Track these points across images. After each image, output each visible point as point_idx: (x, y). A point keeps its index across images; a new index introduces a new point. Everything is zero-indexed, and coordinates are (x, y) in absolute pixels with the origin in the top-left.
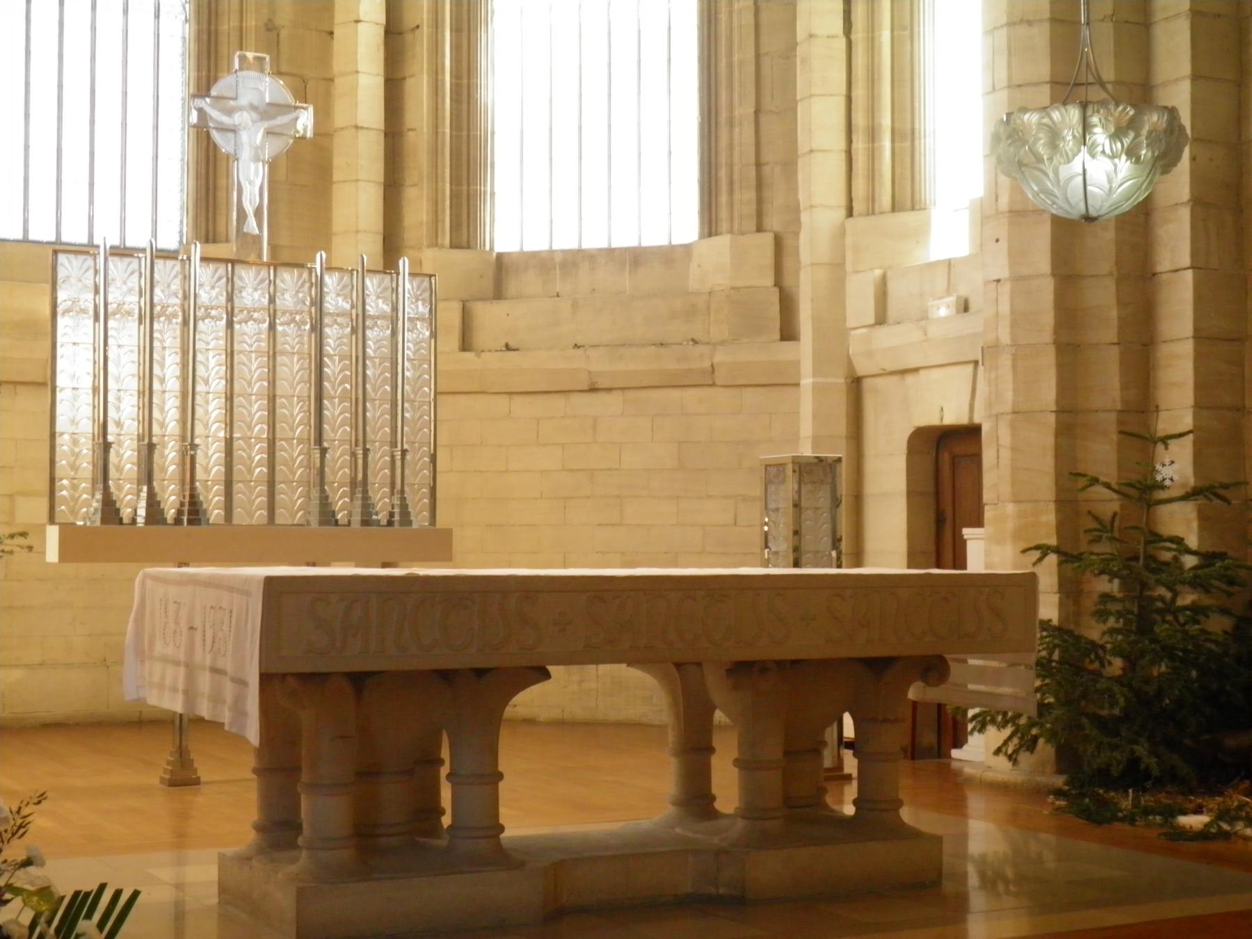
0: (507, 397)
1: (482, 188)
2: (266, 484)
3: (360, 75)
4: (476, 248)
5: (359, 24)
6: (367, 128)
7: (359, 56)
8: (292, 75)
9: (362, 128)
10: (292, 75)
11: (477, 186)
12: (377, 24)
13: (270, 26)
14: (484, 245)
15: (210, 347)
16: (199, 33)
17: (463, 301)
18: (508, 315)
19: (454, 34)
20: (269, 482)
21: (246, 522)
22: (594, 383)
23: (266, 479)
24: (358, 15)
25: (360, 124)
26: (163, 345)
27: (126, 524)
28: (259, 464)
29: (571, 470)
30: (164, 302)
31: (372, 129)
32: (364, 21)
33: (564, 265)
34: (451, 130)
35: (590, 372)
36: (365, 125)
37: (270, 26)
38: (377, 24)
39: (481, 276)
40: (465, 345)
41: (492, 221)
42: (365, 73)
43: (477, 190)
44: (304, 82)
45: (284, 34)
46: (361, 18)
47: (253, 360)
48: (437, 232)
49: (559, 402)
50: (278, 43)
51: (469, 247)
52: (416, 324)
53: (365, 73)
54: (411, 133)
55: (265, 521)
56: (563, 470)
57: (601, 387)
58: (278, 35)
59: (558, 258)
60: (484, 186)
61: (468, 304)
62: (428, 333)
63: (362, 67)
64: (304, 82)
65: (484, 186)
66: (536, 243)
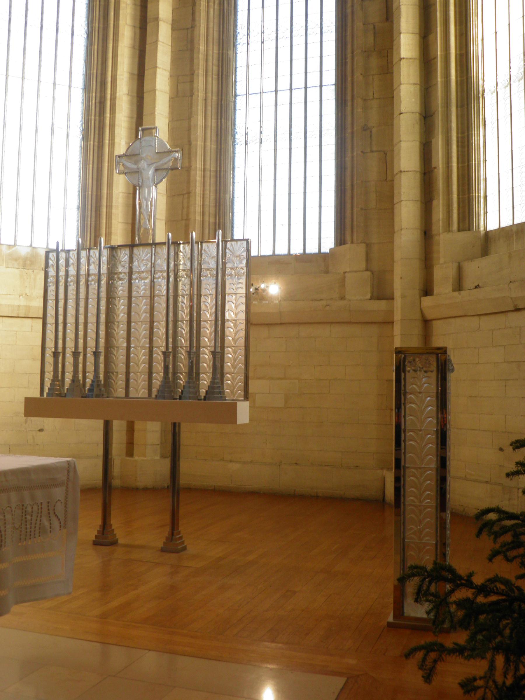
0: (477, 318)
1: (477, 194)
3: (402, 142)
4: (473, 230)
5: (401, 115)
6: (407, 171)
7: (401, 132)
8: (379, 151)
9: (404, 171)
10: (379, 151)
11: (473, 193)
12: (413, 113)
13: (365, 128)
14: (479, 228)
17: (458, 262)
18: (479, 267)
19: (459, 108)
22: (515, 306)
24: (400, 110)
25: (402, 169)
28: (143, 362)
29: (508, 362)
31: (410, 171)
32: (404, 113)
33: (517, 233)
34: (458, 163)
35: (511, 298)
36: (406, 170)
37: (365, 128)
38: (413, 113)
39: (474, 246)
40: (459, 286)
41: (486, 212)
42: (405, 141)
43: (473, 196)
44: (385, 154)
45: (374, 130)
46: (402, 112)
48: (449, 224)
49: (501, 318)
50: (371, 136)
51: (469, 230)
53: (405, 141)
54: (436, 170)
56: (505, 362)
57: (520, 307)
58: (371, 132)
59: (514, 229)
60: (478, 193)
61: (461, 264)
63: (403, 137)
64: (385, 154)
65: (478, 193)
66: (506, 222)
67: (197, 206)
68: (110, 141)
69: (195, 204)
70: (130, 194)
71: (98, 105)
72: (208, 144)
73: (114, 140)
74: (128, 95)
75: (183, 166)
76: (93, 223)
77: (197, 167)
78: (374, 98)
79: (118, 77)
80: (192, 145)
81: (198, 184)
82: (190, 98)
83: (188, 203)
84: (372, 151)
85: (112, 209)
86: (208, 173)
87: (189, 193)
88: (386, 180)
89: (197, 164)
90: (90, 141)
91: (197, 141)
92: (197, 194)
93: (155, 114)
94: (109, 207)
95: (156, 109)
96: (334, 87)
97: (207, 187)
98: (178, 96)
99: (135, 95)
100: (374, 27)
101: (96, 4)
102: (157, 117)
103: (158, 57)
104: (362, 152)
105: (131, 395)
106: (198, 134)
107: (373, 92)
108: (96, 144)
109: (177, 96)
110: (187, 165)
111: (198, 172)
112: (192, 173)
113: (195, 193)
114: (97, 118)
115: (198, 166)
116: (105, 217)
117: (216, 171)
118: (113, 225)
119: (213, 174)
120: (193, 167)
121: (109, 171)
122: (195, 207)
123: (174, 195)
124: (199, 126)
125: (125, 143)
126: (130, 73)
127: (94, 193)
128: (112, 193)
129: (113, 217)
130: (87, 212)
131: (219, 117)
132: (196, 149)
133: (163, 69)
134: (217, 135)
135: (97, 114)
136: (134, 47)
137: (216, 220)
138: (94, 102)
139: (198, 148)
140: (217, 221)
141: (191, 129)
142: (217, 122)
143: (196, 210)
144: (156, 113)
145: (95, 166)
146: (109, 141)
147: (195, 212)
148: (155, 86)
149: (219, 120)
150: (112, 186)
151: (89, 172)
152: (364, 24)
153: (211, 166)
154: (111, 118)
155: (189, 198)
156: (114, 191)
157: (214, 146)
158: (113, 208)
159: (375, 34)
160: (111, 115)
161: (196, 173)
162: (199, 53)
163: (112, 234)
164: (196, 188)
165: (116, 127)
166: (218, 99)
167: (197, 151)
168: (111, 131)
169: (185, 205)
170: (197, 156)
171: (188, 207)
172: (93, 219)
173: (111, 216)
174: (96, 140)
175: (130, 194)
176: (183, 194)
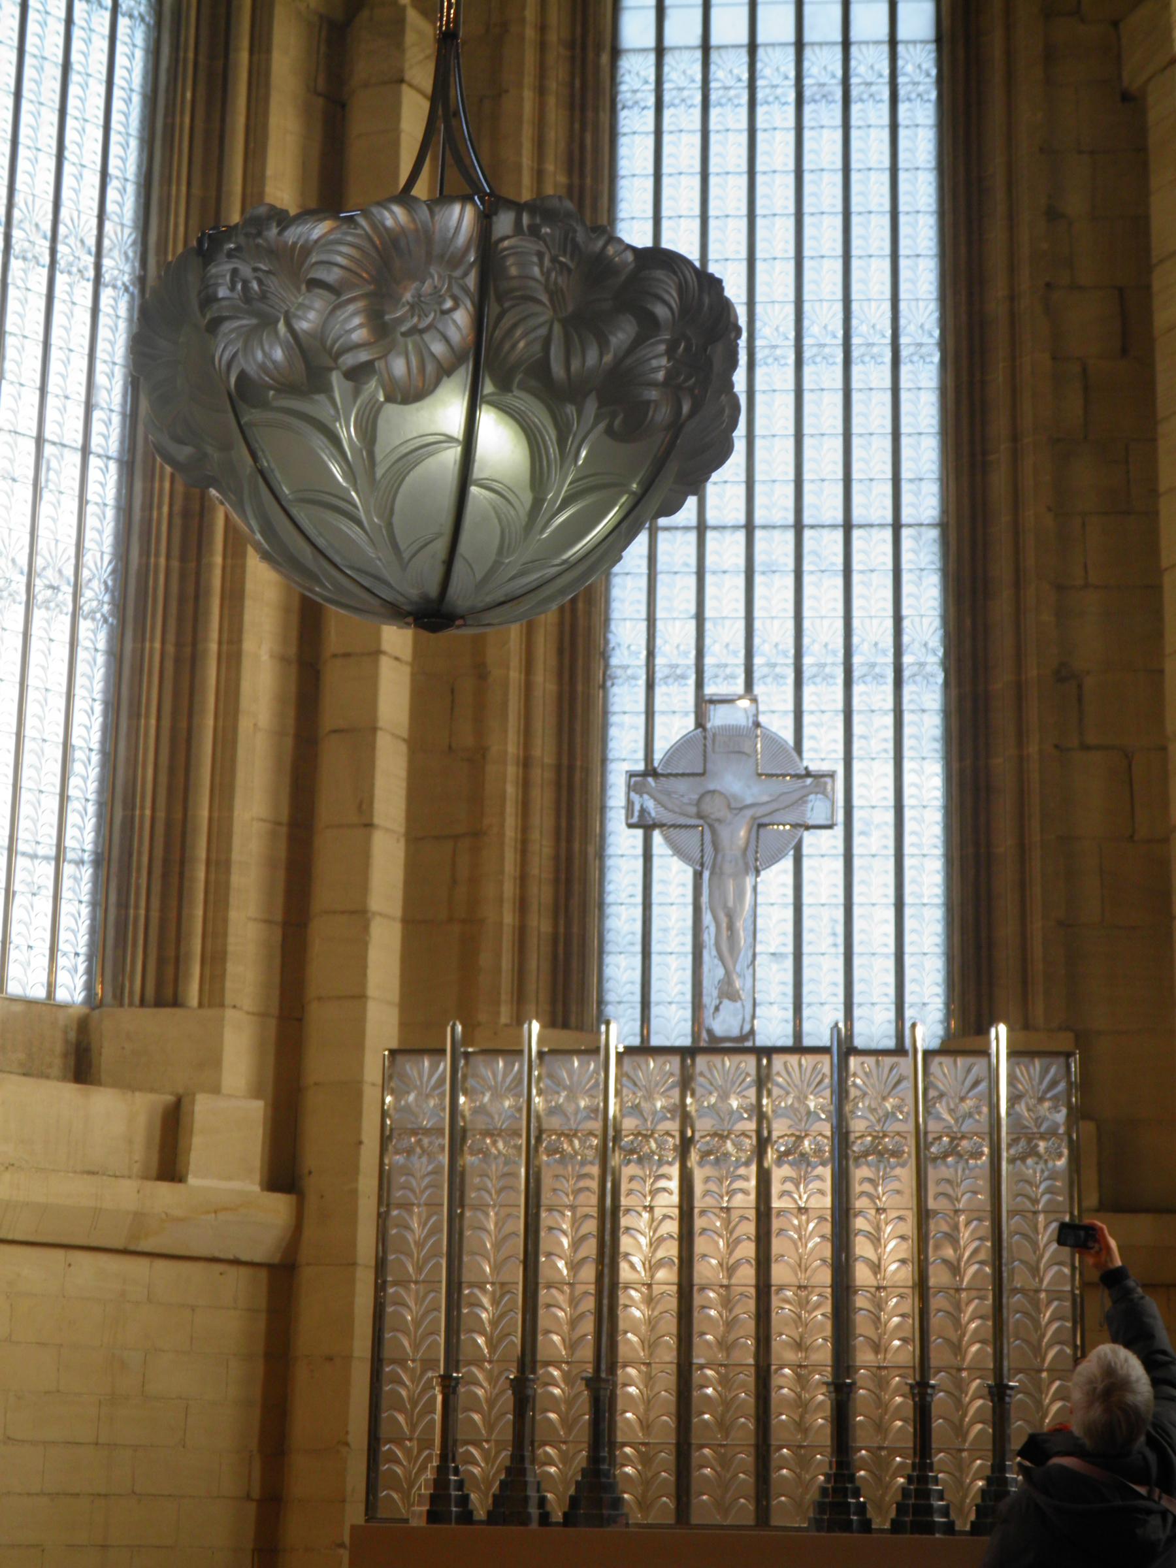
2: (752, 1450)
13: (1064, 675)
15: (961, 1206)
16: (961, 698)
20: (757, 1447)
21: (718, 1519)
23: (752, 1441)
26: (875, 1203)
27: (481, 1522)
30: (955, 1129)
37: (1064, 675)
47: (1041, 1226)
50: (1080, 699)
52: (1037, 1146)
55: (750, 1520)
58: (1080, 687)
62: (1061, 1163)
68: (224, 647)
69: (502, 872)
70: (279, 824)
71: (177, 521)
73: (239, 641)
76: (155, 915)
77: (505, 752)
78: (1086, 586)
84: (1085, 747)
85: (228, 871)
87: (477, 834)
88: (1132, 837)
89: (506, 744)
90: (152, 640)
91: (508, 668)
94: (220, 864)
96: (934, 533)
100: (1084, 370)
101: (178, 191)
104: (1056, 746)
105: (776, 1521)
107: (1085, 566)
108: (171, 649)
112: (491, 769)
113: (501, 835)
114: (175, 564)
116: (200, 896)
117: (558, 768)
118: (232, 929)
119: (549, 775)
120: (494, 749)
122: (501, 883)
127: (161, 815)
128: (230, 818)
129: (233, 901)
130: (138, 878)
132: (506, 694)
134: (560, 651)
135: (176, 552)
137: (556, 926)
138: (165, 509)
140: (562, 930)
145: (166, 723)
146: (220, 643)
147: (501, 900)
150: (231, 797)
151: (146, 742)
152: (1054, 358)
153: (544, 750)
154: (228, 570)
156: (236, 813)
157: (552, 687)
158: (235, 869)
159: (1086, 389)
160: (229, 561)
163: (229, 956)
165: (248, 603)
168: (226, 612)
172: (156, 903)
173: (227, 895)
174: (171, 637)
175: (279, 824)
176: (456, 838)
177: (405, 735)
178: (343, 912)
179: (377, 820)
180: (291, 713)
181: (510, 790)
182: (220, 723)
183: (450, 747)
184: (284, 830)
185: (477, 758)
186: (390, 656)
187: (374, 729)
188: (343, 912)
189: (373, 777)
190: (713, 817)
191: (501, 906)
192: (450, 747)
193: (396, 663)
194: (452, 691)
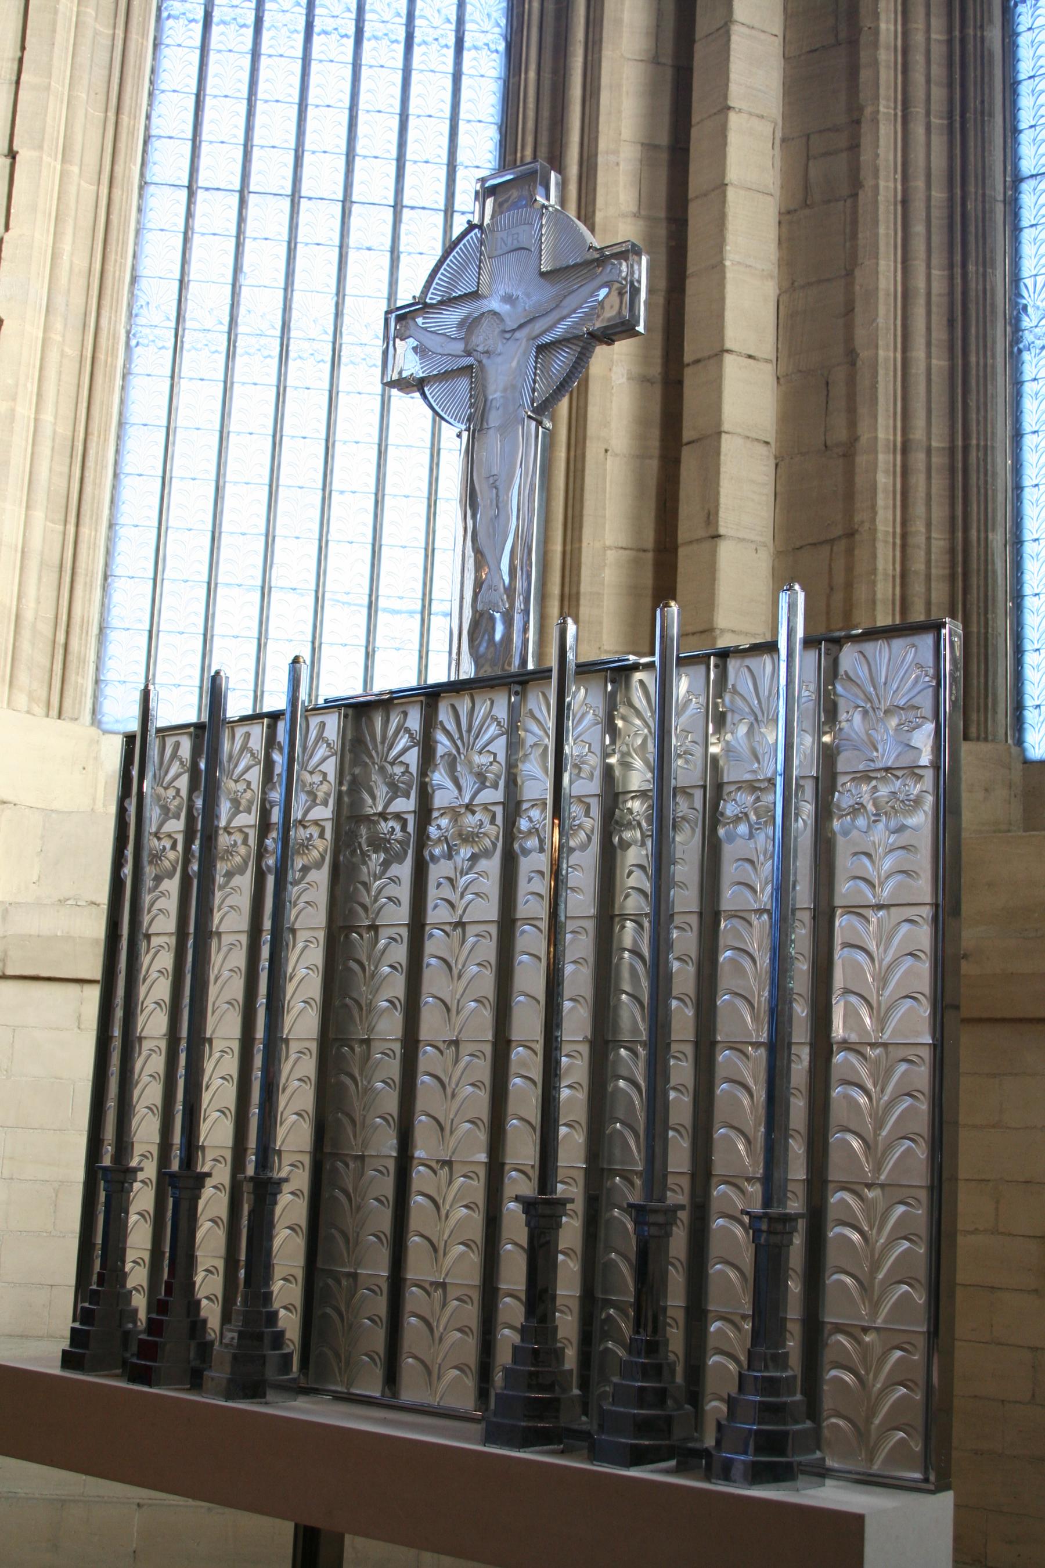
67: (880, 577)
69: (874, 571)
70: (644, 551)
72: (919, 353)
74: (636, 216)
75: (829, 443)
77: (876, 438)
79: (601, 159)
80: (859, 363)
81: (883, 501)
82: (849, 202)
83: (850, 569)
85: (578, 605)
86: (919, 458)
87: (851, 534)
89: (876, 430)
91: (877, 347)
92: (880, 536)
93: (724, 266)
95: (728, 248)
97: (919, 509)
98: (808, 202)
99: (662, 214)
102: (729, 275)
103: (733, 76)
106: (881, 320)
109: (805, 205)
110: (841, 434)
111: (881, 457)
112: (861, 460)
113: (873, 531)
115: (881, 435)
117: (952, 450)
119: (939, 460)
121: (571, 474)
122: (874, 583)
123: (801, 547)
124: (881, 295)
125: (629, 379)
126: (642, 144)
128: (580, 549)
131: (958, 258)
133: (750, 114)
134: (951, 322)
136: (655, 60)
139: (881, 372)
141: (853, 310)
142: (951, 278)
143: (874, 593)
144: (727, 263)
147: (874, 602)
148: (723, 173)
149: (958, 271)
155: (850, 551)
156: (584, 544)
158: (582, 601)
161: (876, 458)
162: (875, 44)
164: (875, 513)
166: (951, 199)
167: (877, 382)
169: (839, 579)
170: (877, 398)
171: (849, 586)
175: (644, 551)
176: (831, 542)
177: (771, 436)
178: (693, 634)
179: (722, 531)
180: (656, 433)
181: (883, 480)
182: (572, 454)
183: (826, 446)
184: (650, 556)
185: (848, 452)
186: (740, 354)
187: (719, 433)
188: (693, 634)
189: (718, 485)
190: (480, 349)
191: (874, 609)
192: (826, 446)
193: (751, 361)
194: (827, 383)
